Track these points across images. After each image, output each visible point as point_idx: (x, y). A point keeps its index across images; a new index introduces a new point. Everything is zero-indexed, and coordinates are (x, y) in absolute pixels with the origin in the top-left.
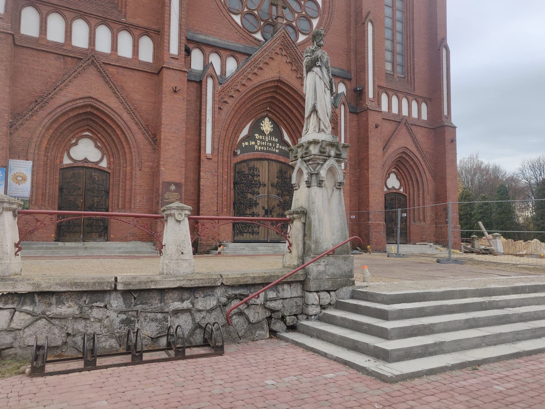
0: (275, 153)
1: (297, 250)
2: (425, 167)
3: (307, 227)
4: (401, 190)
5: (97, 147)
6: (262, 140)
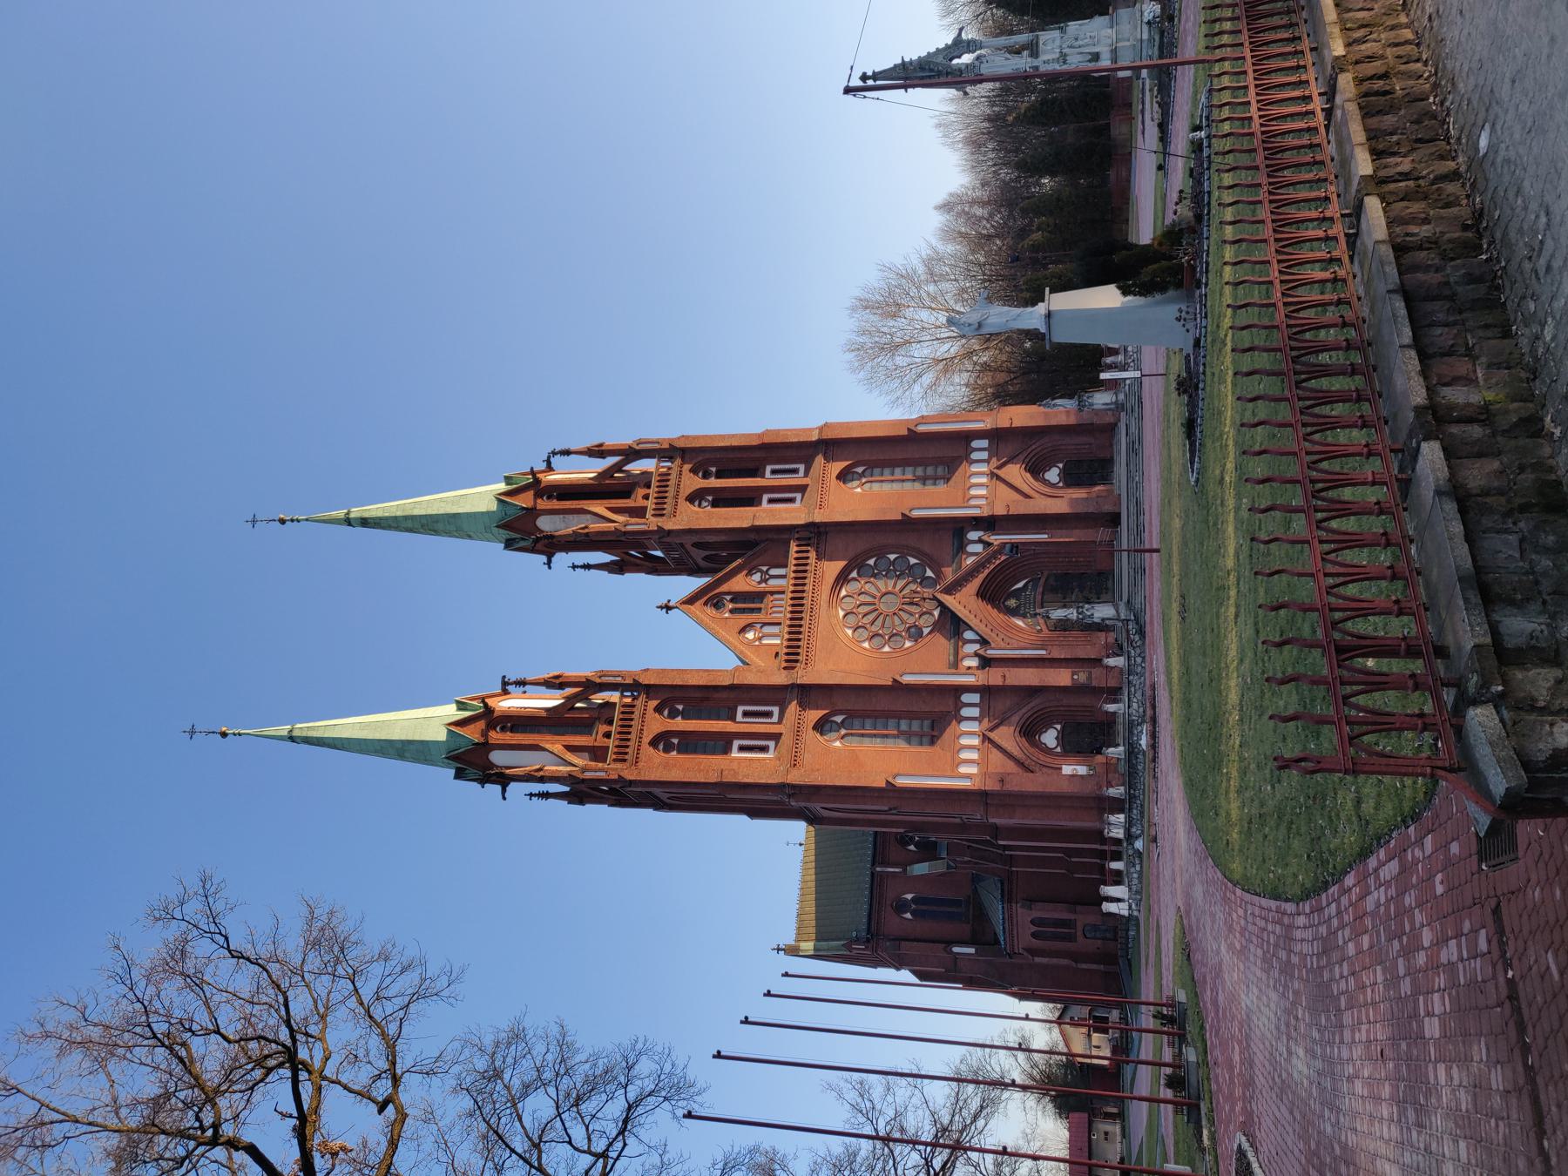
1: (1117, 622)
2: (1038, 444)
4: (1061, 465)
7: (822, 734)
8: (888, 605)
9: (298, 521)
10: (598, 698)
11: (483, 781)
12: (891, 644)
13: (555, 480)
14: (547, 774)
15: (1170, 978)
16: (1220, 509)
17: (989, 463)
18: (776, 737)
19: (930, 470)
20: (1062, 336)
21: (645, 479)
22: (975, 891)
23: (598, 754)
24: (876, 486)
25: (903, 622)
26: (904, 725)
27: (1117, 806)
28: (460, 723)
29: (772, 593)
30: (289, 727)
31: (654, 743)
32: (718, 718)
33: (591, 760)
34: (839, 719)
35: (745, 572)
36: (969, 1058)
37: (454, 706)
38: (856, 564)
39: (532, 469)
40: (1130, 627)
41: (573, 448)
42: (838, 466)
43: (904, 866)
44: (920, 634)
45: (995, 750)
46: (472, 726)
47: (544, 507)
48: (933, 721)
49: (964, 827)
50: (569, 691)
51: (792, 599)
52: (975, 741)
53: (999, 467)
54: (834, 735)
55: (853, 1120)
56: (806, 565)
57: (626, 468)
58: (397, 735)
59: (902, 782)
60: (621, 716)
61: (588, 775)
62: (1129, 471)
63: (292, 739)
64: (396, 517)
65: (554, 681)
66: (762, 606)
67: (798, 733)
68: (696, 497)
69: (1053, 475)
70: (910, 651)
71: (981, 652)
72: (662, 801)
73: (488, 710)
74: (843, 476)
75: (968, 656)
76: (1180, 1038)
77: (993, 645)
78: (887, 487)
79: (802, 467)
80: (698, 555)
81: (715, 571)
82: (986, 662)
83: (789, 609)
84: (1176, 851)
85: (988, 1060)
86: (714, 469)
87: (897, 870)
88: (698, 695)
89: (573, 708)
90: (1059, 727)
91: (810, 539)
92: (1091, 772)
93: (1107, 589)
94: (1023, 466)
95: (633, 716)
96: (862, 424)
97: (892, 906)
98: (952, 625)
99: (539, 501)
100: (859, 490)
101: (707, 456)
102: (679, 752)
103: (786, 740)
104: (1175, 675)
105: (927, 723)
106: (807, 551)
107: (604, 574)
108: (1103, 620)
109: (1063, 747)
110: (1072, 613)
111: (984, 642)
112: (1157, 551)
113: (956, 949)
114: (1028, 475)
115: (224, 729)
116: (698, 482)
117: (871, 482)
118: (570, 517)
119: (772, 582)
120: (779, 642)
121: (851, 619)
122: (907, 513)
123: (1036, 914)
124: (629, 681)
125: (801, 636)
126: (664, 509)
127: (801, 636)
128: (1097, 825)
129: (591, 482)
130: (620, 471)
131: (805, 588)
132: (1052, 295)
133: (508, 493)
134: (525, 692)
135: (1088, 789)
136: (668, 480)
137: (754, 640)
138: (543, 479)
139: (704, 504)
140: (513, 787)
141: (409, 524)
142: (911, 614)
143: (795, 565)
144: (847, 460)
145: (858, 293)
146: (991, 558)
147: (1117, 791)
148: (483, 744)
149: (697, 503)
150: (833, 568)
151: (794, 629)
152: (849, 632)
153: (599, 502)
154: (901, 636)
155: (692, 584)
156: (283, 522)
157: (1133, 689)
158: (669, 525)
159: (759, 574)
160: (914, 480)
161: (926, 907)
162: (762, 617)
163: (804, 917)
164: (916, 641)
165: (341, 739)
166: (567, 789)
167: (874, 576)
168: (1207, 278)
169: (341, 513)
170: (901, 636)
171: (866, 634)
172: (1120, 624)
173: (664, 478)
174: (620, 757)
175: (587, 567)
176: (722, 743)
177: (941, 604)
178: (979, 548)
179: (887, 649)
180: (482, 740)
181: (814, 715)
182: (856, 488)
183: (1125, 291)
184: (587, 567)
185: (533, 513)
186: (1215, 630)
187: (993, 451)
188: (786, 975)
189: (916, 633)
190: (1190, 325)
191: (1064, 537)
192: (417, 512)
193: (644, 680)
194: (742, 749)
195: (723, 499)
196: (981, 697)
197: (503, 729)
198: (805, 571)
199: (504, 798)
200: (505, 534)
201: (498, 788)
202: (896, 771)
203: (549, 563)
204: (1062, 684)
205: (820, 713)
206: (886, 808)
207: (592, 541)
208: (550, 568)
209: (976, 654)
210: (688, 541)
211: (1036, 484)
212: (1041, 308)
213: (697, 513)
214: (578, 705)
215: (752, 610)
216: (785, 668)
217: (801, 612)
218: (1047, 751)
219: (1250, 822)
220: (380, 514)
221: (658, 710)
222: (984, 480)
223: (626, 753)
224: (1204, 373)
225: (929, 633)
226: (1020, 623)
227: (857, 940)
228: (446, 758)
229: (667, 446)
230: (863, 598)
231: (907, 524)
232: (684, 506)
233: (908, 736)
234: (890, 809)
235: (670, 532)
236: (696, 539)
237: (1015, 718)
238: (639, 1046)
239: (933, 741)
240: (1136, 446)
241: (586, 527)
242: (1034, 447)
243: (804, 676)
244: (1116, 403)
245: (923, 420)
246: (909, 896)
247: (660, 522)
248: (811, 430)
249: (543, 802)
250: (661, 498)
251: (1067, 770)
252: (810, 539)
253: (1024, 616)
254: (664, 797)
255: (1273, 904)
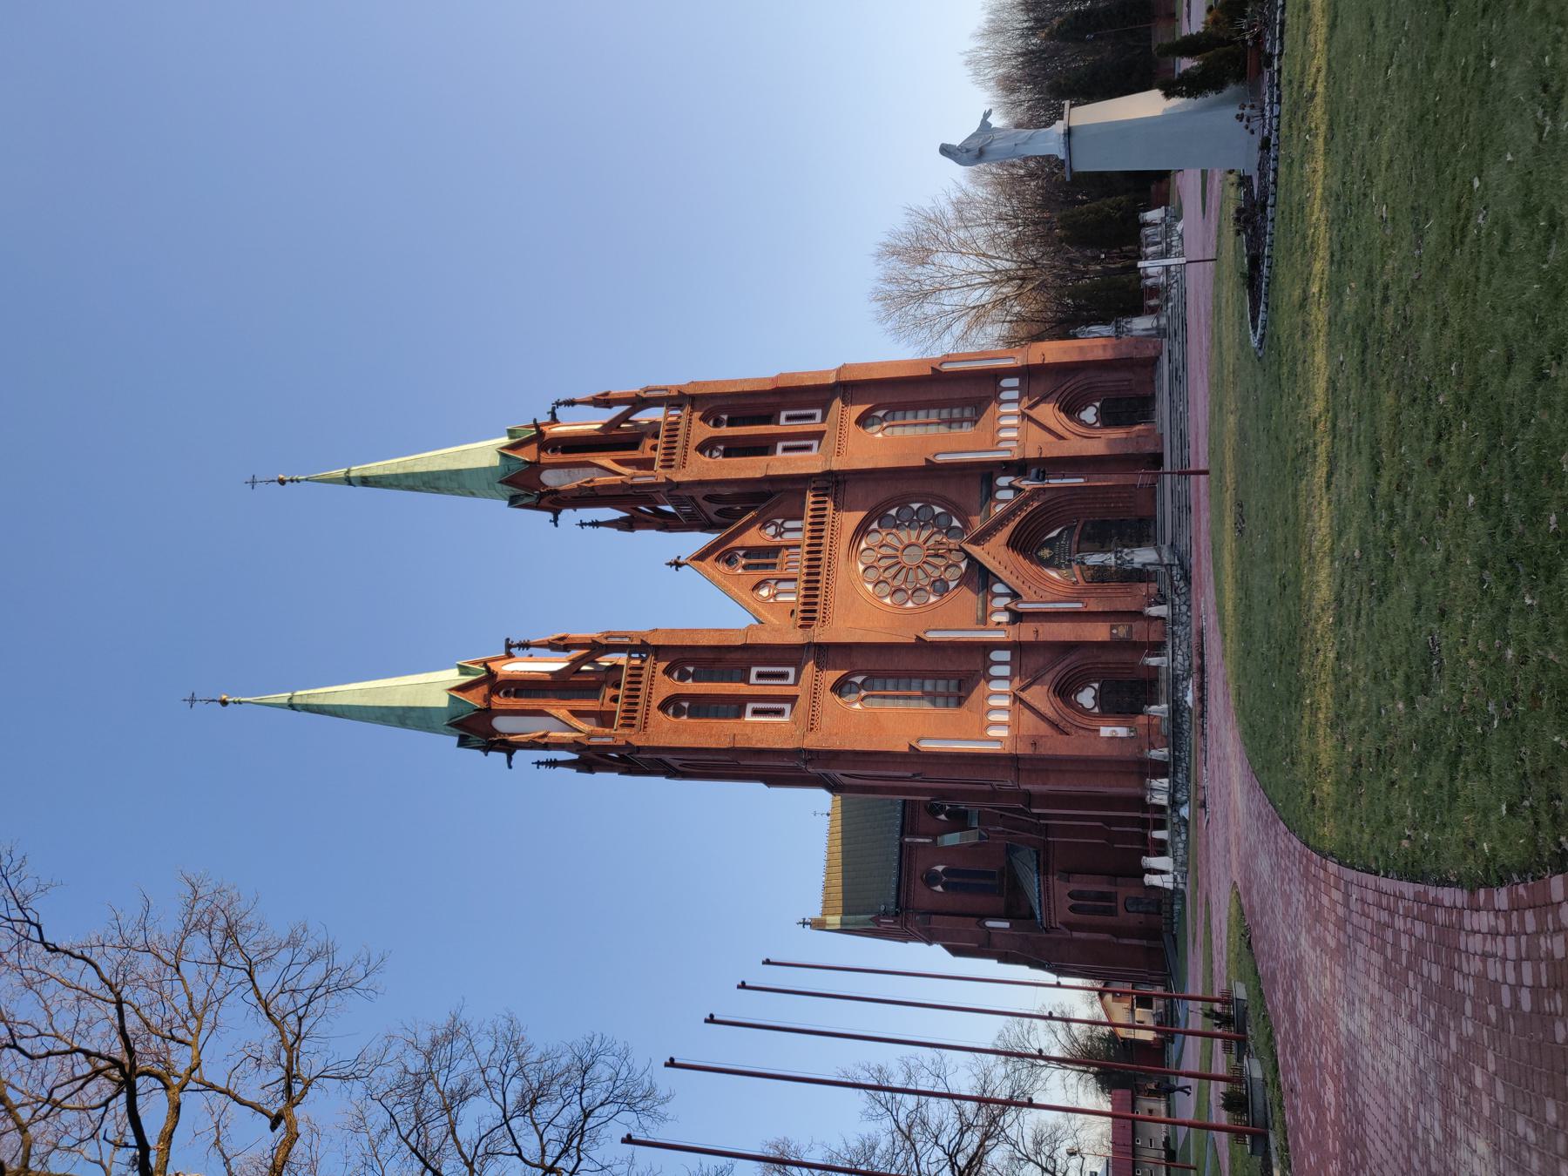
0: (1070, 544)
2: (1072, 382)
3: (1150, 564)
4: (1098, 404)
5: (1082, 691)
6: (1060, 558)
7: (840, 696)
8: (911, 558)
9: (298, 481)
10: (606, 661)
11: (487, 748)
12: (914, 599)
13: (561, 433)
14: (551, 740)
15: (1224, 964)
16: (1300, 346)
17: (1019, 403)
18: (792, 700)
19: (956, 413)
20: (1085, 163)
21: (653, 429)
22: (1010, 863)
23: (605, 719)
24: (898, 431)
25: (927, 575)
26: (929, 685)
27: (1160, 769)
28: (462, 688)
29: (787, 547)
30: (289, 694)
31: (663, 707)
32: (731, 681)
33: (598, 726)
34: (858, 680)
35: (758, 526)
36: (1007, 1034)
37: (456, 671)
38: (877, 515)
39: (535, 420)
40: (1174, 572)
41: (578, 398)
42: (857, 410)
43: (935, 836)
44: (947, 589)
45: (1027, 712)
46: (474, 691)
47: (548, 461)
48: (960, 681)
49: (994, 795)
50: (575, 653)
51: (808, 553)
52: (1006, 702)
53: (1030, 408)
54: (853, 697)
55: (870, 1111)
56: (823, 516)
57: (633, 418)
58: (398, 701)
59: (927, 746)
60: (629, 679)
61: (595, 741)
62: (1172, 401)
63: (292, 706)
64: (396, 475)
65: (558, 642)
66: (777, 561)
67: (814, 695)
68: (706, 447)
69: (1089, 415)
70: (935, 606)
71: (1012, 606)
72: (674, 769)
73: (491, 675)
74: (863, 421)
75: (998, 610)
76: (1239, 1044)
77: (1024, 598)
78: (909, 431)
79: (818, 413)
80: (711, 509)
81: (726, 526)
82: (1017, 617)
83: (806, 563)
84: (1231, 819)
85: (1026, 1037)
86: (725, 417)
87: (927, 841)
88: (711, 656)
89: (578, 671)
90: (1096, 686)
91: (827, 488)
92: (1132, 734)
93: (1148, 536)
94: (1057, 405)
95: (641, 679)
96: (883, 365)
97: (922, 878)
98: (980, 577)
99: (543, 454)
100: (880, 435)
101: (719, 402)
102: (690, 716)
103: (802, 702)
104: (1229, 606)
105: (953, 683)
106: (825, 502)
107: (614, 531)
108: (1144, 565)
109: (1101, 708)
110: (1110, 559)
111: (1015, 595)
112: (1206, 472)
113: (990, 924)
114: (1062, 415)
115: (224, 697)
116: (709, 431)
117: (893, 426)
118: (575, 471)
119: (787, 536)
120: (794, 599)
121: (872, 573)
122: (931, 458)
123: (1073, 887)
124: (637, 642)
125: (818, 593)
126: (673, 460)
127: (818, 593)
128: (1138, 791)
129: (597, 433)
130: (627, 421)
131: (822, 541)
132: (1073, 109)
133: (511, 447)
134: (531, 656)
135: (1129, 752)
136: (677, 429)
137: (769, 597)
138: (548, 432)
139: (716, 454)
140: (519, 755)
141: (410, 482)
142: (936, 567)
143: (812, 517)
144: (866, 403)
145: (885, 239)
146: (1022, 504)
147: (1160, 754)
148: (485, 710)
149: (707, 453)
150: (852, 519)
151: (810, 585)
152: (870, 587)
153: (605, 454)
154: (926, 591)
155: (700, 540)
156: (282, 482)
157: (1177, 641)
158: (679, 476)
159: (773, 528)
160: (939, 424)
161: (958, 880)
162: (777, 573)
163: (832, 889)
164: (942, 595)
165: (341, 706)
166: (575, 757)
167: (897, 527)
168: (1282, 45)
169: (341, 472)
170: (926, 591)
171: (887, 589)
172: (1163, 570)
173: (673, 428)
174: (628, 722)
175: (596, 524)
176: (734, 707)
177: (968, 556)
178: (1009, 494)
179: (910, 604)
180: (484, 706)
181: (832, 676)
182: (877, 433)
183: (1168, 95)
184: (596, 524)
185: (536, 467)
186: (1291, 519)
187: (1024, 390)
188: (767, 962)
189: (940, 587)
190: (1255, 125)
191: (1099, 481)
192: (418, 469)
193: (653, 641)
194: (756, 712)
195: (734, 448)
196: (1012, 655)
197: (507, 694)
198: (823, 523)
199: (510, 767)
200: (510, 490)
201: (504, 756)
202: (919, 735)
203: (555, 521)
204: (1100, 639)
205: (839, 674)
206: (910, 775)
207: (597, 496)
208: (556, 525)
209: (1007, 609)
210: (699, 493)
211: (1071, 424)
212: (1059, 127)
213: (707, 463)
214: (585, 668)
215: (766, 566)
216: (801, 627)
217: (818, 566)
218: (1084, 712)
219: (1358, 765)
220: (380, 472)
221: (668, 672)
222: (1014, 421)
223: (634, 718)
224: (1275, 183)
225: (956, 587)
226: (1054, 575)
227: (886, 914)
228: (449, 725)
229: (675, 393)
230: (884, 551)
231: (932, 470)
232: (694, 456)
233: (932, 697)
234: (914, 775)
235: (679, 484)
236: (707, 491)
237: (1049, 677)
238: (596, 1045)
239: (959, 704)
240: (1180, 373)
241: (592, 481)
242: (1068, 384)
243: (821, 634)
244: (1157, 328)
245: (948, 358)
246: (940, 868)
247: (669, 473)
248: (828, 372)
249: (550, 771)
250: (670, 449)
251: (1105, 732)
252: (827, 488)
253: (1058, 567)
254: (676, 764)
255: (1408, 889)
